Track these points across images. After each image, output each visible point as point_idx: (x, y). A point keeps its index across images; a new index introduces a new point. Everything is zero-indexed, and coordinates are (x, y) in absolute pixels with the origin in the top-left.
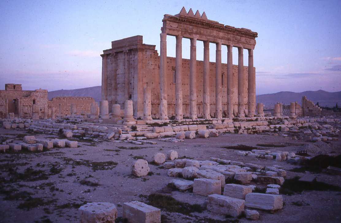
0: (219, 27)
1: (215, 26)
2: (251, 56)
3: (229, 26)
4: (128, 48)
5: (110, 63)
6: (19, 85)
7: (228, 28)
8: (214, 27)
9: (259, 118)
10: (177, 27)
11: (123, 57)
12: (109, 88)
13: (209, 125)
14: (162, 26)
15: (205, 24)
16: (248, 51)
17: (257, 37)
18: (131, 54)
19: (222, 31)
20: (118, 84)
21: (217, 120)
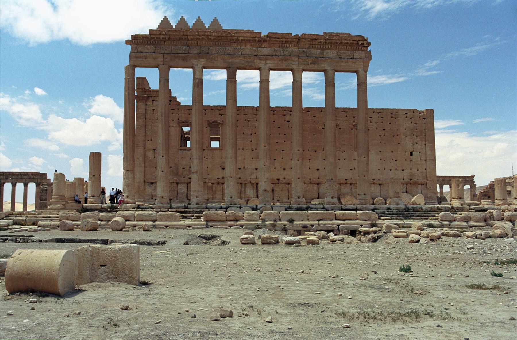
1: (240, 38)
15: (212, 38)
17: (369, 44)
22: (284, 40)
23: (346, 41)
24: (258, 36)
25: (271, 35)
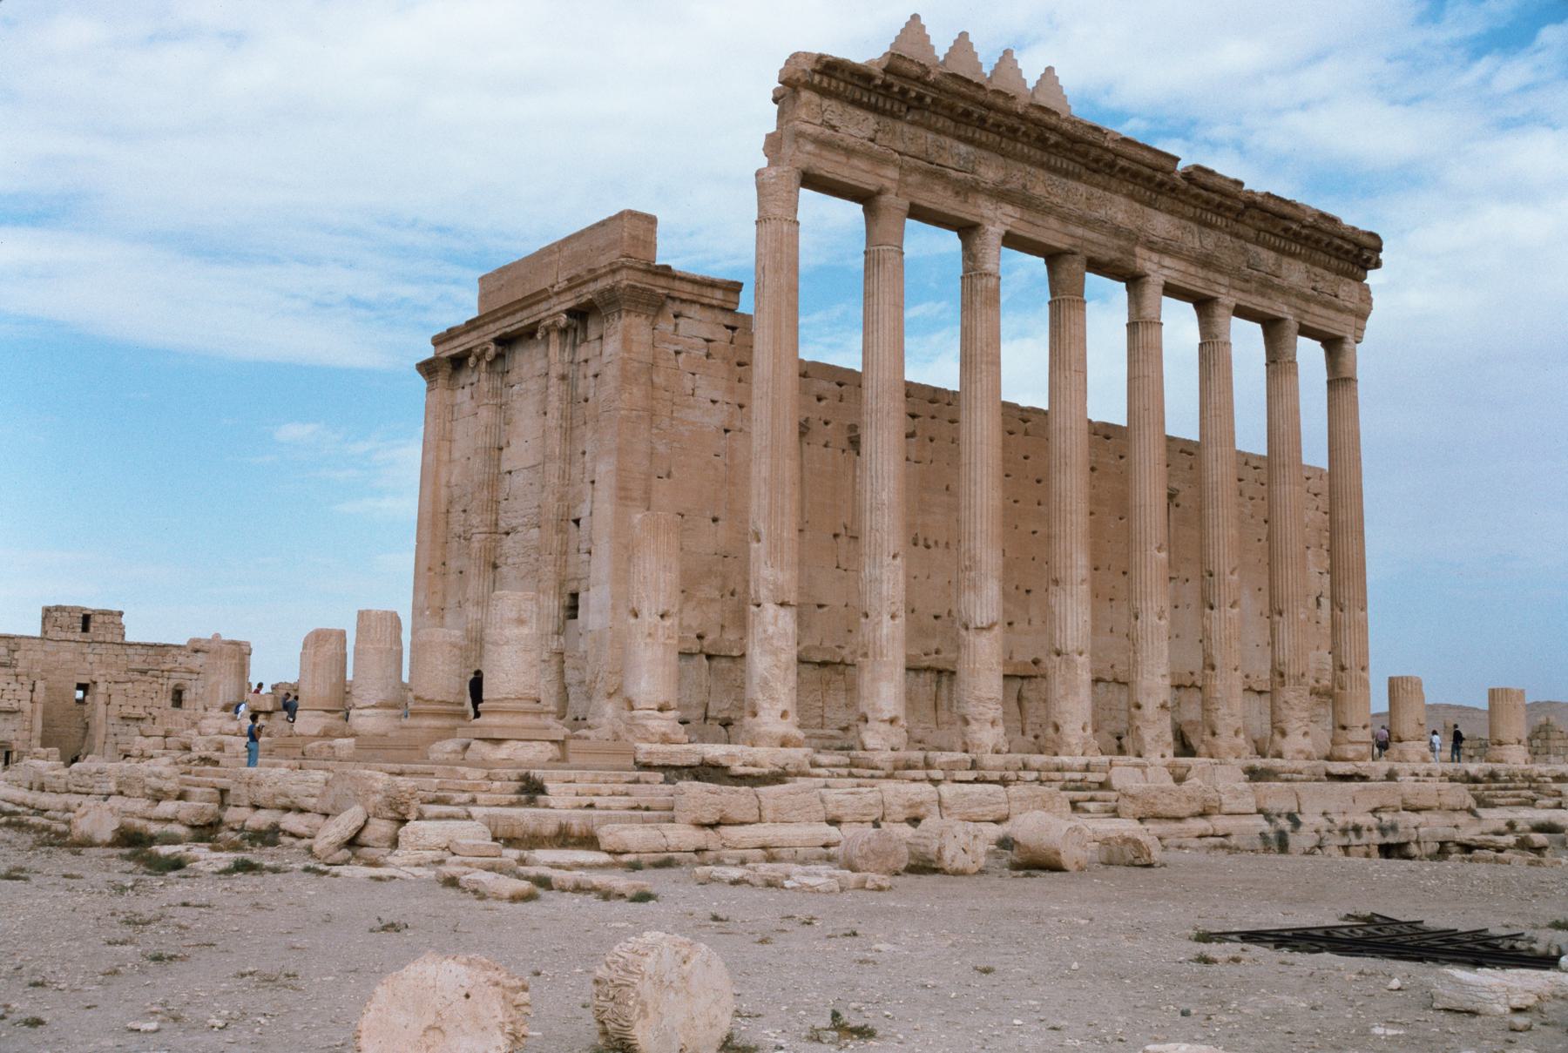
0: (1148, 171)
1: (1122, 163)
2: (1340, 381)
3: (1211, 173)
4: (569, 301)
5: (468, 406)
6: (110, 613)
7: (1206, 188)
8: (1111, 165)
9: (1405, 766)
10: (872, 140)
11: (540, 364)
12: (454, 565)
13: (1086, 792)
14: (772, 127)
15: (1053, 138)
16: (1322, 351)
17: (1378, 265)
18: (585, 340)
19: (1164, 201)
20: (508, 534)
21: (1143, 767)
22: (1217, 198)
23: (1338, 242)
24: (1169, 166)
25: (1196, 174)
